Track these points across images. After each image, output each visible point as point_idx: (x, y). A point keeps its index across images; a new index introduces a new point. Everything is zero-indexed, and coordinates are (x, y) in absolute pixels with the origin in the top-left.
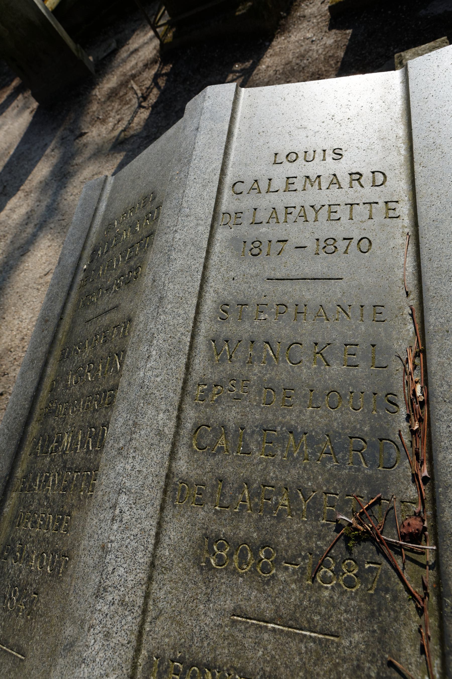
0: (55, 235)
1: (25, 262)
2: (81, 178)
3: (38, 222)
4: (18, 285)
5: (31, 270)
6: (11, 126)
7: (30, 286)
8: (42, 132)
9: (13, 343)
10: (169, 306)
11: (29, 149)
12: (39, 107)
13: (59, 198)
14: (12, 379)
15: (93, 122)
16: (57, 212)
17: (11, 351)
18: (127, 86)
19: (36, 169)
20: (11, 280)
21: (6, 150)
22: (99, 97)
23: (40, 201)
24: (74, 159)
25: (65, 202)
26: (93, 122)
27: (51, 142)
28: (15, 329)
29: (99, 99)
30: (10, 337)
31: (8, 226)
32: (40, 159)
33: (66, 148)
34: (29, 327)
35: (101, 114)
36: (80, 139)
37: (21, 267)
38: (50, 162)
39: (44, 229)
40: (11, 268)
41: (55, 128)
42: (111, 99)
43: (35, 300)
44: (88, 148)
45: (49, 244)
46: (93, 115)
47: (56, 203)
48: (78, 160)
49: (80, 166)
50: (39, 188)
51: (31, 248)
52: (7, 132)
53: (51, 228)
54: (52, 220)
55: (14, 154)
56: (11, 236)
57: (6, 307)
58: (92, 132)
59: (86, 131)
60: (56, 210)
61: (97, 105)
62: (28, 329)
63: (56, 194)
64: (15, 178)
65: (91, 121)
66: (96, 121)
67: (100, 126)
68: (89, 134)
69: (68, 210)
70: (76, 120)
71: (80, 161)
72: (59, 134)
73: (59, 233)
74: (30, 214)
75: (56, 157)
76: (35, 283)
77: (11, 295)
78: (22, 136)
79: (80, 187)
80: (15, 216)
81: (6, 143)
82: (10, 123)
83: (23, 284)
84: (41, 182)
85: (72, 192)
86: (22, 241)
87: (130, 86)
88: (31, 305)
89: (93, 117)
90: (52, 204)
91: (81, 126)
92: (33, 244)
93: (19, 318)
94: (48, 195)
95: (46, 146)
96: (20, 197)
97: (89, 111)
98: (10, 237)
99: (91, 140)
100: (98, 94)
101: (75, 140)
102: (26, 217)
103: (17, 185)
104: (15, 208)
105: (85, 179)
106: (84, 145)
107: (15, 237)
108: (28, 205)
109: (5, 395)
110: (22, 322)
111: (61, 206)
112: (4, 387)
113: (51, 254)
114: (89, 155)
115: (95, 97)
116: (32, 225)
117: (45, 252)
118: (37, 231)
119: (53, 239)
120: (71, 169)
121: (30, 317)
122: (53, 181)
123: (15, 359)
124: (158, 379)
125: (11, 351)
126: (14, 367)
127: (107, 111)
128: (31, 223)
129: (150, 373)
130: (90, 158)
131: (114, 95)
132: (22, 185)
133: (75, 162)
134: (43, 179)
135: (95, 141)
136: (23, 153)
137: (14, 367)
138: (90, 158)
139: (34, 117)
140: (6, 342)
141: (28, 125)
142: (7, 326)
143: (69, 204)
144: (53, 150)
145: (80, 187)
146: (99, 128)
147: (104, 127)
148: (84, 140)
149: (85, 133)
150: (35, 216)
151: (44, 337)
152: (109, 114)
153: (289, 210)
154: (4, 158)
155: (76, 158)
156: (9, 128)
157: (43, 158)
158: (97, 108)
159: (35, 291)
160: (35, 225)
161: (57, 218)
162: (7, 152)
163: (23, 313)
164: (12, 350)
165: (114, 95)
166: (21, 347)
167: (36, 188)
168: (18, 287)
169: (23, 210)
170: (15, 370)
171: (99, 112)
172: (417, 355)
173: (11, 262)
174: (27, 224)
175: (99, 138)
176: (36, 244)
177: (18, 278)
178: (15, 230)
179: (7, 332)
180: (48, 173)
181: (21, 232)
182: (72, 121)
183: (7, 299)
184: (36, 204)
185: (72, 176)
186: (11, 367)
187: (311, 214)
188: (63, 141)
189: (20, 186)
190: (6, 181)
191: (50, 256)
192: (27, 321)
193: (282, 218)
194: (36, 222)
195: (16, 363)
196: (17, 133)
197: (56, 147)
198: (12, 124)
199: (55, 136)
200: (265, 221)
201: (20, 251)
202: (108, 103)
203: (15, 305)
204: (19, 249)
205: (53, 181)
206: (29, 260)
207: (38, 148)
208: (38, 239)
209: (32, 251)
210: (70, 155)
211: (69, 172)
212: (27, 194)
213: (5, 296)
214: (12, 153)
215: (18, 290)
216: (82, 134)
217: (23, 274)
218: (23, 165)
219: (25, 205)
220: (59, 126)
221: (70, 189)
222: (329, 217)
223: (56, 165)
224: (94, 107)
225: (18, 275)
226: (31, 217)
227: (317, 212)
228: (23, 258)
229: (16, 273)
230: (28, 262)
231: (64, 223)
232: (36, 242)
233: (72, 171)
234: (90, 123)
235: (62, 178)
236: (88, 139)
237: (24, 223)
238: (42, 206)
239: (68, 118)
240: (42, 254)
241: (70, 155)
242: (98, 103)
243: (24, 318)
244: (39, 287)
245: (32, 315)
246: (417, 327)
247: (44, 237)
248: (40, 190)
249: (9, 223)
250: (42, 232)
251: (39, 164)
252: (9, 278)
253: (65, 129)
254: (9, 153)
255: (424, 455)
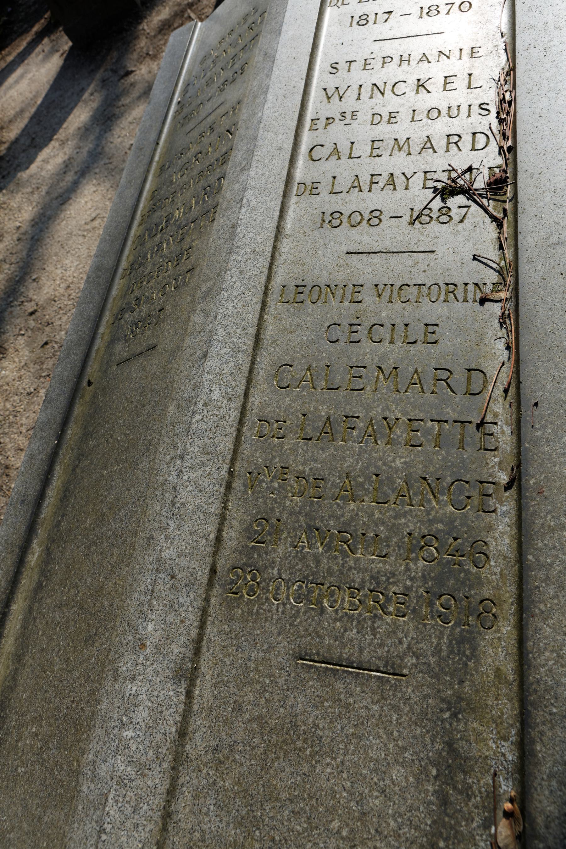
0: (102, 180)
1: (65, 210)
2: (130, 119)
3: (79, 169)
4: (59, 234)
5: (75, 218)
6: (37, 73)
7: (75, 233)
8: (76, 76)
9: (56, 293)
10: (283, 65)
11: (61, 96)
12: (71, 48)
13: (104, 142)
14: (58, 328)
15: (141, 59)
16: (101, 156)
17: (55, 301)
18: (182, 16)
19: (72, 116)
20: (50, 230)
21: (31, 99)
22: (148, 31)
23: (80, 148)
24: (120, 100)
25: (112, 145)
26: (142, 59)
27: (89, 85)
28: (58, 278)
29: (148, 34)
30: (53, 287)
31: (41, 178)
32: (76, 105)
33: (108, 90)
34: (75, 275)
35: (151, 49)
36: (126, 78)
37: (62, 216)
38: (90, 107)
39: (87, 175)
40: (49, 218)
41: (92, 71)
42: (163, 32)
43: (80, 247)
44: (137, 87)
45: (95, 189)
46: (141, 51)
47: (100, 147)
48: (125, 100)
49: (128, 107)
50: (77, 135)
51: (73, 196)
52: (32, 80)
53: (96, 173)
54: (96, 165)
55: (43, 103)
56: (46, 188)
57: (45, 258)
58: (141, 69)
59: (133, 69)
60: (100, 154)
61: (146, 40)
62: (74, 277)
63: (99, 138)
64: (45, 128)
65: (139, 59)
66: (144, 58)
67: (150, 62)
68: (138, 72)
69: (115, 152)
70: (119, 59)
71: (128, 101)
72: (99, 76)
73: (106, 177)
74: (68, 162)
75: (97, 101)
76: (79, 230)
77: (52, 245)
78: (51, 82)
79: (129, 127)
80: (49, 167)
81: (31, 92)
82: (34, 70)
83: (65, 232)
84: (79, 129)
85: (119, 133)
86: (60, 191)
87: (186, 15)
88: (76, 253)
89: (141, 54)
90: (95, 149)
91: (126, 65)
92: (75, 191)
93: (62, 267)
94: (89, 141)
95: (83, 90)
96: (54, 147)
97: (136, 48)
98: (44, 189)
99: (140, 78)
100: (146, 27)
101: (119, 80)
102: (63, 166)
103: (49, 135)
104: (48, 159)
105: (135, 119)
106: (131, 84)
107: (51, 187)
108: (65, 154)
109: (51, 344)
110: (66, 270)
111: (107, 149)
112: (50, 336)
113: (97, 199)
114: (138, 94)
115: (142, 32)
116: (72, 173)
117: (89, 197)
118: (79, 178)
119: (99, 184)
120: (117, 111)
121: (75, 264)
122: (95, 125)
123: (60, 308)
124: (276, 114)
125: (55, 301)
126: (59, 316)
127: (158, 46)
128: (70, 171)
129: (268, 111)
130: (139, 98)
131: (167, 27)
132: (56, 134)
133: (120, 103)
134: (82, 125)
135: (144, 79)
136: (54, 101)
137: (59, 316)
138: (139, 98)
139: (66, 60)
140: (48, 293)
141: (58, 69)
142: (48, 276)
143: (116, 147)
144: (92, 94)
145: (129, 127)
146: (149, 65)
147: (156, 63)
148: (131, 78)
149: (132, 72)
150: (75, 164)
151: (140, 162)
152: (161, 48)
153: (375, 179)
154: (30, 109)
155: (122, 99)
156: (34, 76)
157: (80, 104)
158: (146, 43)
159: (81, 239)
160: (76, 173)
161: (102, 163)
162: (33, 102)
163: (67, 262)
164: (56, 299)
165: (167, 27)
166: (67, 296)
167: (73, 135)
168: (59, 236)
169: (59, 160)
170: (60, 318)
171: (148, 47)
172: (508, 74)
173: (49, 213)
174: (65, 173)
175: (150, 75)
176: (78, 191)
177: (58, 227)
178: (51, 181)
179: (48, 283)
180: (87, 119)
181: (58, 182)
182: (114, 60)
183: (47, 249)
184: (75, 152)
185: (119, 117)
186: (55, 316)
187: (400, 181)
188: (104, 82)
189: (53, 136)
190: (35, 133)
191: (97, 201)
192: (73, 269)
193: (365, 188)
194: (77, 169)
195: (61, 312)
196: (45, 80)
197: (96, 91)
198: (37, 71)
199: (93, 79)
200: (345, 190)
201: (59, 200)
202: (160, 37)
203: (56, 254)
204: (57, 198)
205: (95, 125)
206: (71, 207)
207: (73, 94)
208: (80, 186)
209: (73, 198)
210: (114, 97)
211: (114, 115)
212: (63, 143)
213: (44, 247)
214: (39, 102)
215: (60, 239)
216: (128, 73)
217: (64, 222)
218: (55, 114)
219: (61, 155)
220: (99, 68)
221: (117, 131)
222: (424, 184)
223: (97, 109)
224: (143, 43)
225: (59, 224)
226: (70, 166)
227: (408, 179)
228: (64, 207)
229: (56, 223)
230: (70, 210)
231: (111, 166)
232: (78, 189)
233: (117, 113)
234: (137, 61)
235: (106, 121)
236: (136, 77)
237: (61, 172)
238: (82, 153)
239: (109, 58)
240: (86, 200)
241: (114, 97)
242: (147, 38)
243: (68, 266)
244: (85, 233)
245: (78, 263)
246: (509, 55)
247: (87, 183)
248: (79, 136)
249: (42, 174)
250: (84, 179)
251: (75, 111)
252: (47, 228)
253: (106, 70)
254: (36, 102)
255: (509, 133)
